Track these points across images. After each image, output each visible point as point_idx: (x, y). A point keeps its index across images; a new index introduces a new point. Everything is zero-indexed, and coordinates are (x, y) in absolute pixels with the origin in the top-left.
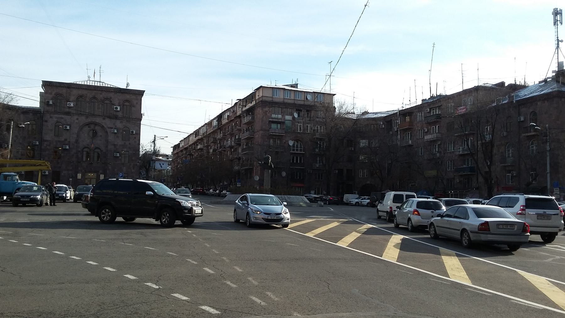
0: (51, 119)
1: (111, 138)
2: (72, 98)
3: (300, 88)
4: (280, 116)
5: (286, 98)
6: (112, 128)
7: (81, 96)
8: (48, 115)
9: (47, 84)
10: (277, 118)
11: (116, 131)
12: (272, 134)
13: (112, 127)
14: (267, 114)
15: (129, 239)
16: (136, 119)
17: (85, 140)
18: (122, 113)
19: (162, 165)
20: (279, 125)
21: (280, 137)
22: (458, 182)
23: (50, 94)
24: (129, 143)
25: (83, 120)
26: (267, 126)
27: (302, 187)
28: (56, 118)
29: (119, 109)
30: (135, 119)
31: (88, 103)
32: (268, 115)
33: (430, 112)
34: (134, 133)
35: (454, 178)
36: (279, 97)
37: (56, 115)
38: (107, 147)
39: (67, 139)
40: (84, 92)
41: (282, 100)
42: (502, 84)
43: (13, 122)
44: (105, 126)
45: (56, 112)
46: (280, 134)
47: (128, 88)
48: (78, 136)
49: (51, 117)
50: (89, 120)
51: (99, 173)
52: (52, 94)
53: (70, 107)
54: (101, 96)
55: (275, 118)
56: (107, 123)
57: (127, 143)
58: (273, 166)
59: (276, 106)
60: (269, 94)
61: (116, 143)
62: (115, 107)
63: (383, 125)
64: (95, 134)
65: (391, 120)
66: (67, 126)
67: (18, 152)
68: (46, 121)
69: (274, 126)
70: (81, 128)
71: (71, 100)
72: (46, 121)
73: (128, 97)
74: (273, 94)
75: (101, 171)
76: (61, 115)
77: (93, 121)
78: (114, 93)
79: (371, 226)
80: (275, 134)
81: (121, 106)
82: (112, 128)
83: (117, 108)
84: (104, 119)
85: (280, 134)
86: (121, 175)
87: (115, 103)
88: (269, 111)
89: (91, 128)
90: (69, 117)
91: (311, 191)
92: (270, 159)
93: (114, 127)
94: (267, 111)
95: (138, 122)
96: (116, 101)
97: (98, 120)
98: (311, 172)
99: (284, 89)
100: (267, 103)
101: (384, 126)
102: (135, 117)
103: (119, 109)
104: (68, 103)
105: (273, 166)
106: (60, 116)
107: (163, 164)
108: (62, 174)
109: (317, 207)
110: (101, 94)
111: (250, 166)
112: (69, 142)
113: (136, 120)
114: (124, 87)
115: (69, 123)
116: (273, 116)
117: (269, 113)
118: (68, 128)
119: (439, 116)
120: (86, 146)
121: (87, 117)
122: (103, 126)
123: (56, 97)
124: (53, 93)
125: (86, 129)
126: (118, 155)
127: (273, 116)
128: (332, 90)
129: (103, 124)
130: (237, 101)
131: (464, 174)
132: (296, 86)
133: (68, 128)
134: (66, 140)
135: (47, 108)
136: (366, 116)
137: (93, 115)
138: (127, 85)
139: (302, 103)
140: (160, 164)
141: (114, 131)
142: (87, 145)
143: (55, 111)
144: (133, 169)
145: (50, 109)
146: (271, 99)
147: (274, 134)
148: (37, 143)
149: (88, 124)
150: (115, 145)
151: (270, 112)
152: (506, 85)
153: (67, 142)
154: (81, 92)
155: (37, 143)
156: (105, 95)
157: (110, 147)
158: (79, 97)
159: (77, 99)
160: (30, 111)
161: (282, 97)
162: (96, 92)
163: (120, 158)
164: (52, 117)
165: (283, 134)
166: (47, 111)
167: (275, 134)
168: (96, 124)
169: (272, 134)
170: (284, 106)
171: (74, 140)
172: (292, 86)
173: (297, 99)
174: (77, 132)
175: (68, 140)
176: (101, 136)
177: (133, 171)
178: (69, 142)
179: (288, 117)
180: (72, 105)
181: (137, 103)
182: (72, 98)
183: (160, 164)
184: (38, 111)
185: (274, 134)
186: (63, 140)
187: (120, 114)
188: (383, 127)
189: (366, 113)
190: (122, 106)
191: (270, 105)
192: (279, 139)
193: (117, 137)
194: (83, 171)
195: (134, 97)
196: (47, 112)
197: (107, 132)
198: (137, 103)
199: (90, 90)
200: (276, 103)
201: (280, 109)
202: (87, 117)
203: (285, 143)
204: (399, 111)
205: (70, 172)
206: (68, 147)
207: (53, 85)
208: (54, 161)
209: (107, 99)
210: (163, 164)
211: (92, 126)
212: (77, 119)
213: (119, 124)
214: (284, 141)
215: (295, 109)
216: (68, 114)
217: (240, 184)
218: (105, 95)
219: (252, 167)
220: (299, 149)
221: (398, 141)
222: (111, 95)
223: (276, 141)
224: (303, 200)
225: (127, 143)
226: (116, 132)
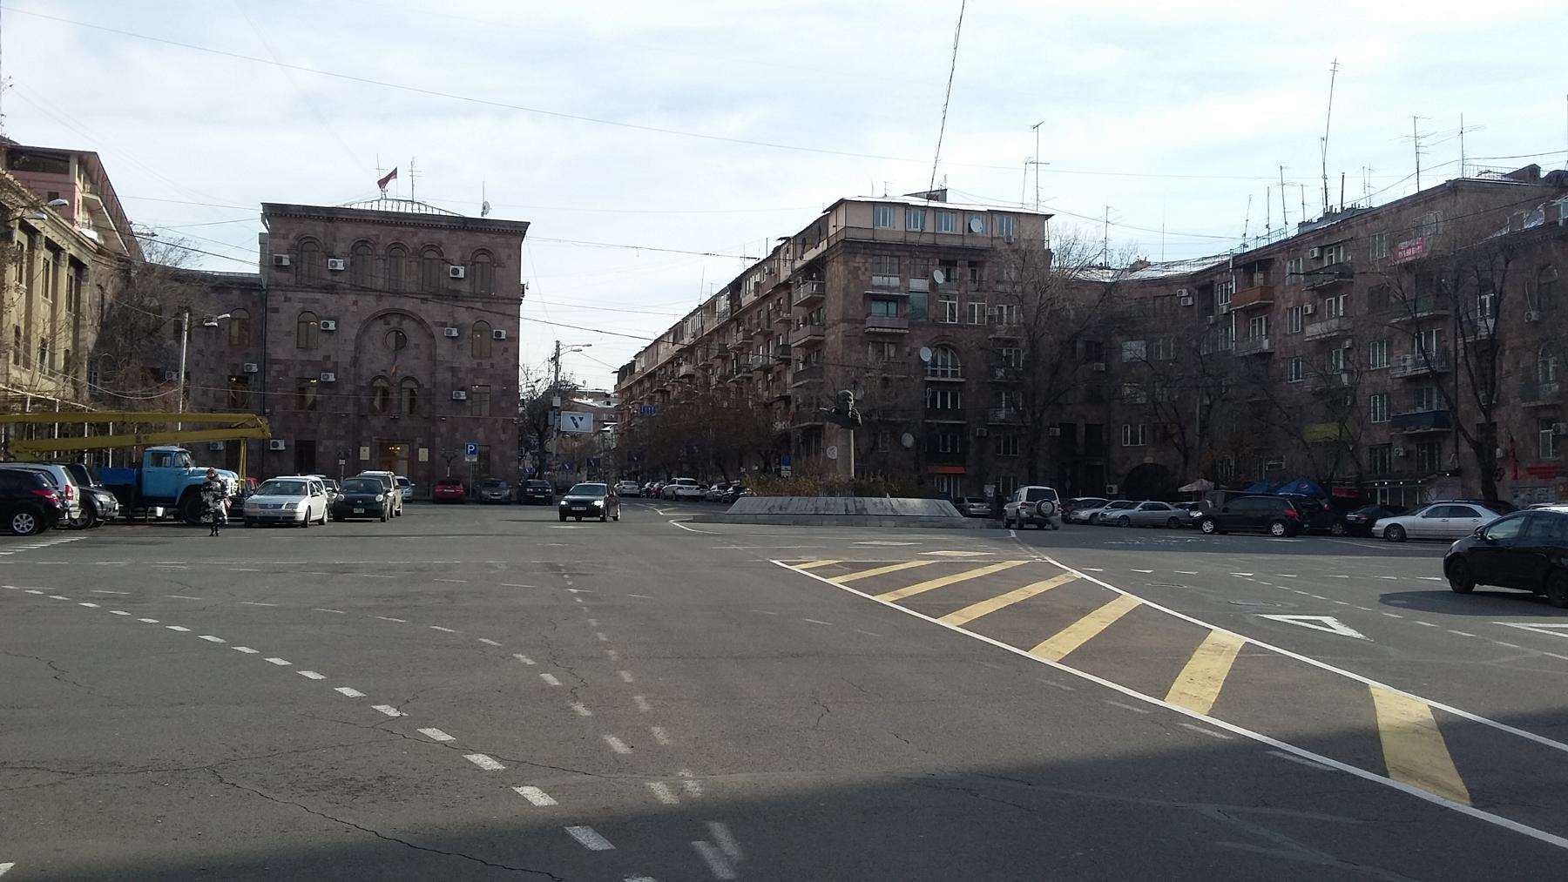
0: (287, 304)
1: (443, 350)
2: (341, 247)
3: (953, 202)
4: (895, 281)
5: (913, 229)
6: (444, 324)
7: (364, 242)
8: (281, 293)
9: (275, 213)
10: (888, 288)
11: (455, 333)
12: (873, 330)
13: (446, 323)
14: (858, 277)
15: (405, 607)
17: (378, 358)
18: (471, 284)
19: (578, 420)
20: (892, 306)
21: (896, 339)
22: (1401, 454)
23: (284, 238)
24: (492, 366)
25: (370, 304)
26: (860, 308)
27: (961, 474)
29: (461, 275)
30: (504, 299)
31: (381, 261)
32: (861, 277)
33: (1320, 258)
34: (503, 337)
35: (1389, 445)
36: (894, 228)
37: (300, 295)
38: (433, 374)
40: (372, 231)
41: (900, 237)
42: (1533, 170)
43: (187, 315)
44: (428, 321)
45: (300, 287)
46: (894, 331)
47: (486, 217)
48: (356, 348)
49: (287, 300)
50: (388, 303)
51: (416, 446)
52: (287, 238)
53: (335, 272)
54: (415, 240)
55: (880, 287)
56: (433, 311)
57: (486, 364)
58: (859, 418)
59: (885, 252)
60: (863, 220)
61: (456, 365)
62: (452, 267)
63: (1190, 299)
64: (401, 340)
65: (1212, 282)
66: (329, 322)
67: (205, 393)
68: (276, 310)
69: (878, 308)
70: (366, 325)
71: (337, 252)
72: (276, 310)
73: (484, 240)
74: (875, 222)
75: (419, 440)
77: (397, 307)
78: (447, 232)
79: (1078, 575)
80: (881, 330)
81: (469, 266)
82: (444, 324)
83: (456, 272)
84: (424, 300)
85: (894, 331)
86: (471, 448)
87: (451, 258)
88: (863, 269)
89: (390, 326)
90: (334, 298)
91: (986, 486)
92: (851, 400)
93: (450, 321)
94: (859, 268)
95: (515, 307)
96: (454, 253)
97: (408, 305)
98: (985, 434)
99: (906, 205)
100: (860, 246)
101: (1193, 300)
102: (504, 295)
103: (461, 275)
104: (330, 260)
105: (859, 418)
106: (311, 296)
107: (581, 419)
108: (321, 449)
109: (981, 528)
110: (415, 234)
111: (815, 421)
112: (336, 363)
113: (506, 301)
114: (474, 213)
115: (332, 314)
116: (877, 280)
117: (863, 274)
118: (332, 326)
119: (1345, 272)
120: (381, 374)
121: (381, 296)
122: (421, 322)
123: (300, 247)
124: (291, 236)
125: (379, 328)
126: (463, 395)
127: (877, 280)
128: (1042, 204)
129: (423, 316)
130: (780, 243)
131: (1418, 431)
132: (941, 195)
133: (332, 326)
134: (327, 358)
135: (277, 275)
136: (1145, 274)
137: (397, 293)
138: (484, 208)
139: (957, 242)
140: (573, 419)
141: (451, 333)
142: (383, 371)
143: (297, 283)
144: (504, 432)
145: (282, 277)
146: (869, 235)
147: (878, 330)
148: (255, 369)
149: (384, 316)
150: (453, 370)
151: (866, 269)
152: (1543, 175)
153: (330, 365)
154: (362, 231)
155: (255, 369)
156: (424, 236)
157: (443, 376)
158: (357, 246)
159: (352, 249)
160: (233, 283)
161: (900, 227)
162: (400, 228)
163: (469, 403)
164: (290, 298)
165: (902, 331)
166: (278, 285)
167: (881, 330)
168: (404, 315)
169: (873, 330)
170: (907, 254)
171: (349, 359)
172: (930, 196)
173: (943, 231)
174: (354, 338)
175: (332, 359)
176: (417, 346)
177: (503, 437)
178: (336, 363)
179: (919, 284)
180: (340, 267)
181: (509, 257)
182: (341, 247)
183: (573, 419)
184: (255, 285)
185: (878, 330)
186: (320, 358)
187: (465, 288)
188: (1190, 303)
189: (1142, 264)
190: (471, 264)
191: (868, 252)
192: (891, 343)
193: (460, 348)
194: (374, 440)
195: (502, 240)
196: (277, 286)
197: (432, 336)
198: (509, 257)
199: (387, 224)
200: (884, 245)
201: (896, 260)
202: (379, 298)
203: (909, 354)
204: (1234, 258)
205: (341, 443)
206: (332, 378)
207: (291, 215)
208: (300, 415)
209: (431, 247)
210: (581, 419)
211: (394, 321)
212: (355, 303)
213: (464, 316)
214: (908, 349)
215: (937, 261)
216: (330, 288)
217: (789, 468)
218: (424, 236)
219: (821, 424)
220: (949, 373)
221: (1233, 341)
222: (442, 236)
223: (886, 349)
224: (943, 511)
225: (486, 364)
226: (457, 335)
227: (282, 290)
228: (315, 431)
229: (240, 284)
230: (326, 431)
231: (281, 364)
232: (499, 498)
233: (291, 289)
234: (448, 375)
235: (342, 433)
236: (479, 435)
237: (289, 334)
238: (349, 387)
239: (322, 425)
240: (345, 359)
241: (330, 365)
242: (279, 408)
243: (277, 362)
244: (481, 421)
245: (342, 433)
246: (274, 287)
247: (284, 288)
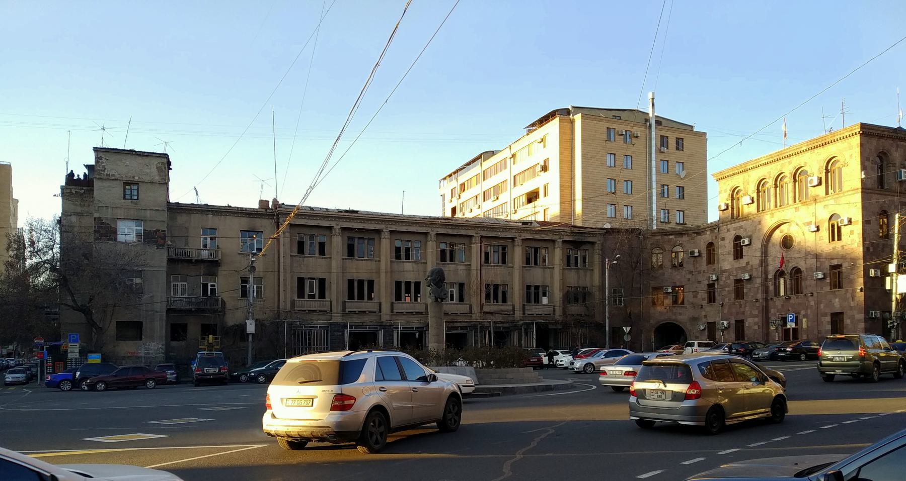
16: (850, 191)
28: (734, 230)
30: (848, 191)
39: (749, 262)
49: (728, 230)
72: (723, 239)
76: (739, 222)
86: (791, 317)
115: (749, 234)
134: (748, 263)
148: (714, 278)
153: (749, 267)
174: (760, 247)
175: (750, 263)
178: (752, 266)
196: (723, 223)
205: (756, 320)
208: (736, 304)
227: (725, 225)
228: (743, 313)
229: (708, 227)
230: (749, 312)
231: (727, 272)
232: (757, 356)
233: (729, 223)
234: (814, 261)
235: (756, 312)
236: (835, 305)
237: (729, 252)
238: (759, 281)
239: (747, 309)
240: (756, 262)
241: (749, 267)
242: (727, 300)
243: (725, 271)
244: (837, 293)
245: (756, 312)
246: (721, 225)
247: (726, 224)
